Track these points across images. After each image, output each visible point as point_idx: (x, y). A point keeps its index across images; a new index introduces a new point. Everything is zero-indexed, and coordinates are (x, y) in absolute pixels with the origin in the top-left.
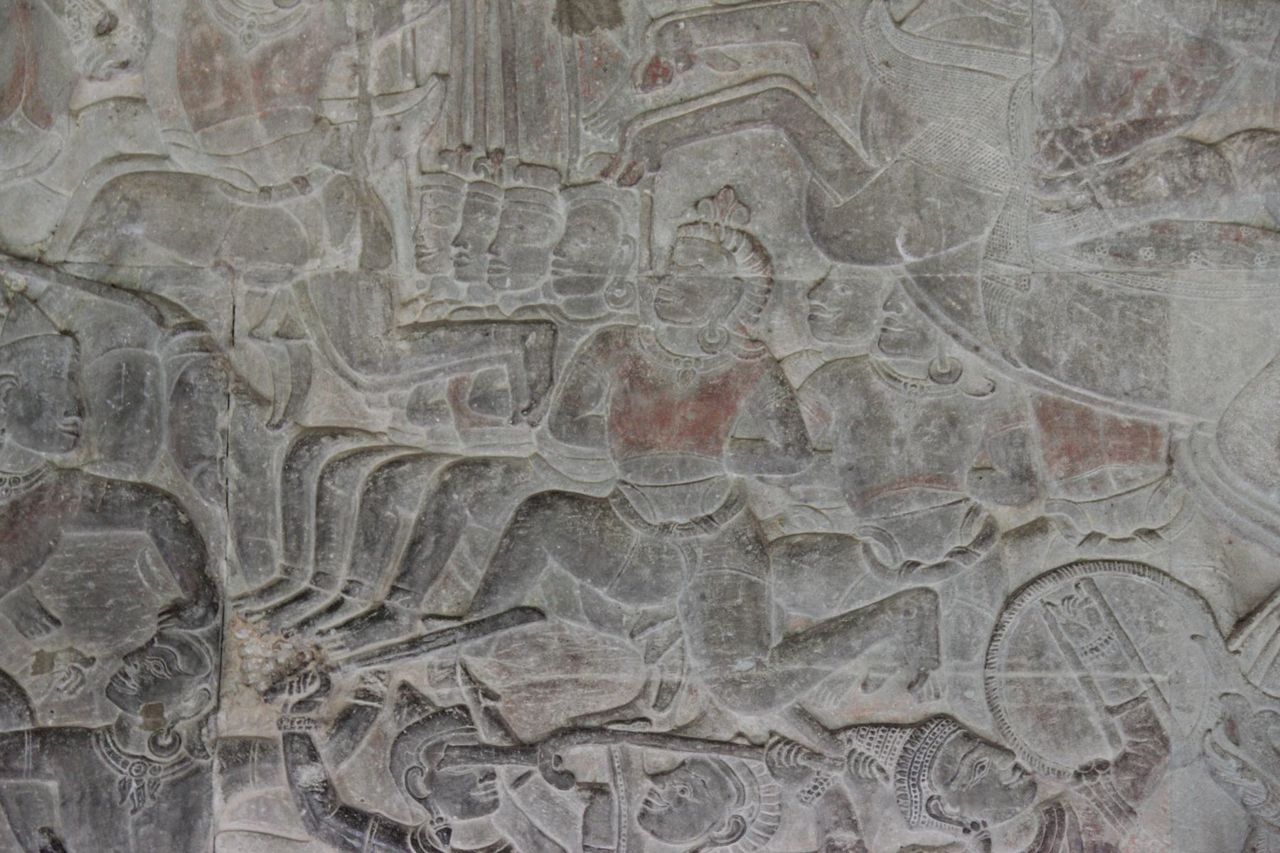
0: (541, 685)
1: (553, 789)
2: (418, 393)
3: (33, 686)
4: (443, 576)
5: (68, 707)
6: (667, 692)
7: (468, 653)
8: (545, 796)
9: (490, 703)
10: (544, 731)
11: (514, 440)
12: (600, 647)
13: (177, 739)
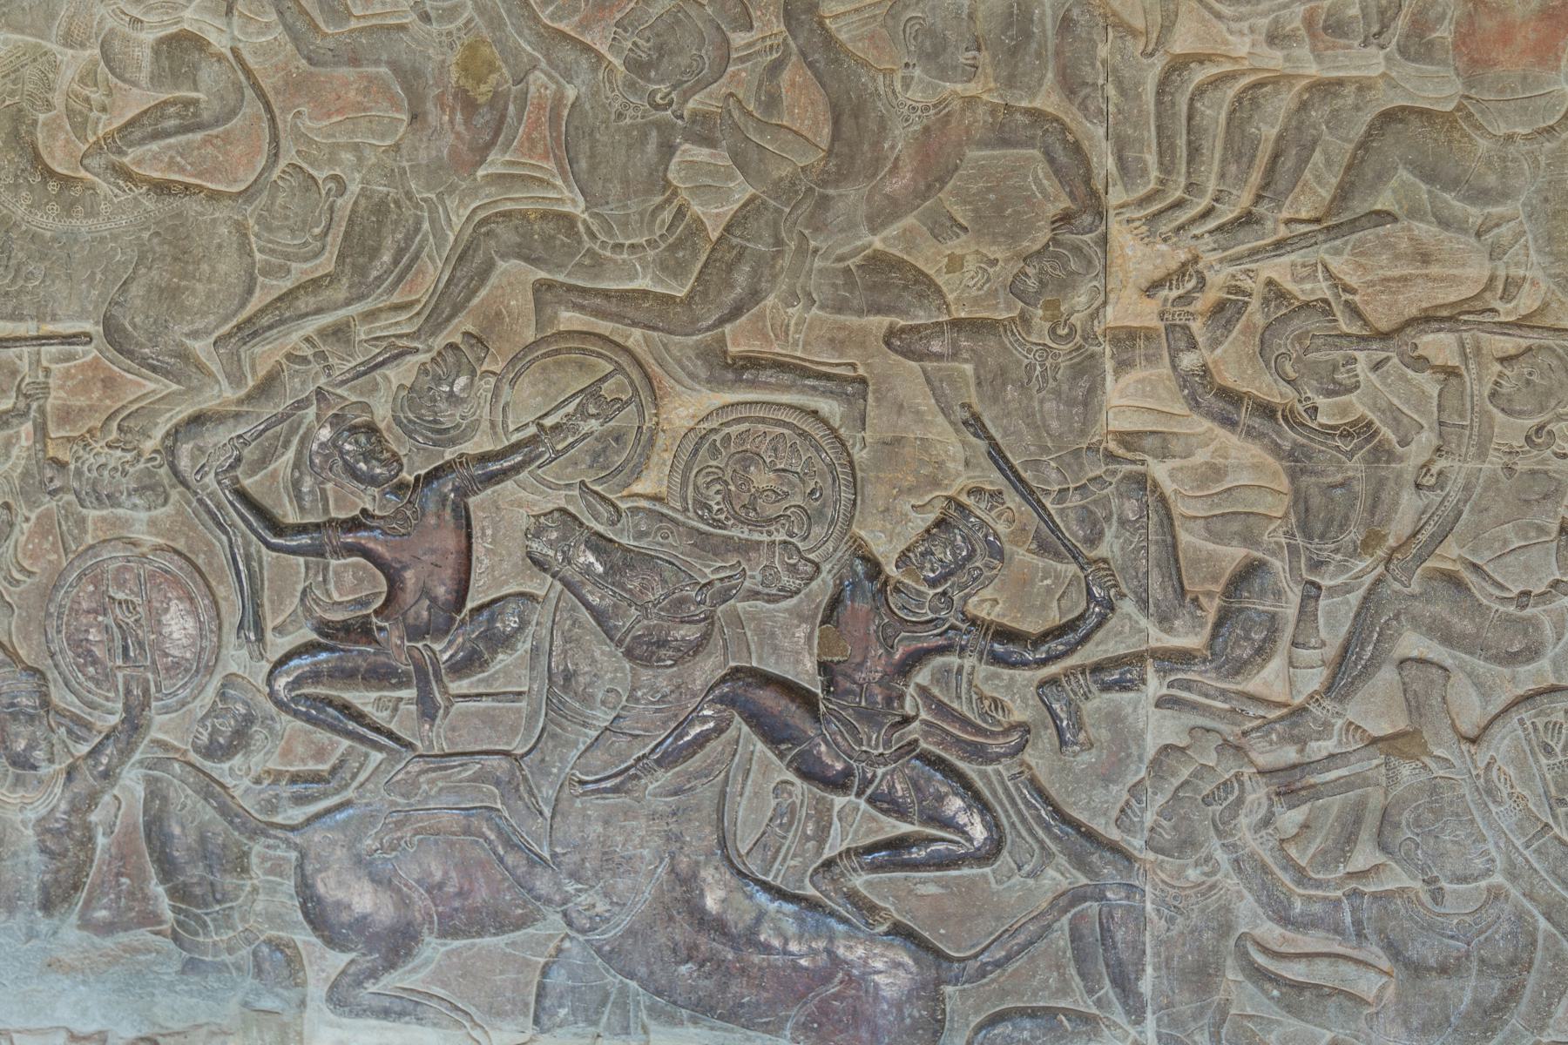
0: (1394, 279)
1: (1410, 373)
2: (1276, 21)
3: (947, 283)
4: (1300, 184)
5: (976, 301)
6: (1511, 287)
7: (1327, 252)
8: (1403, 377)
9: (1350, 297)
10: (1396, 320)
11: (1367, 63)
12: (1447, 246)
13: (1073, 329)
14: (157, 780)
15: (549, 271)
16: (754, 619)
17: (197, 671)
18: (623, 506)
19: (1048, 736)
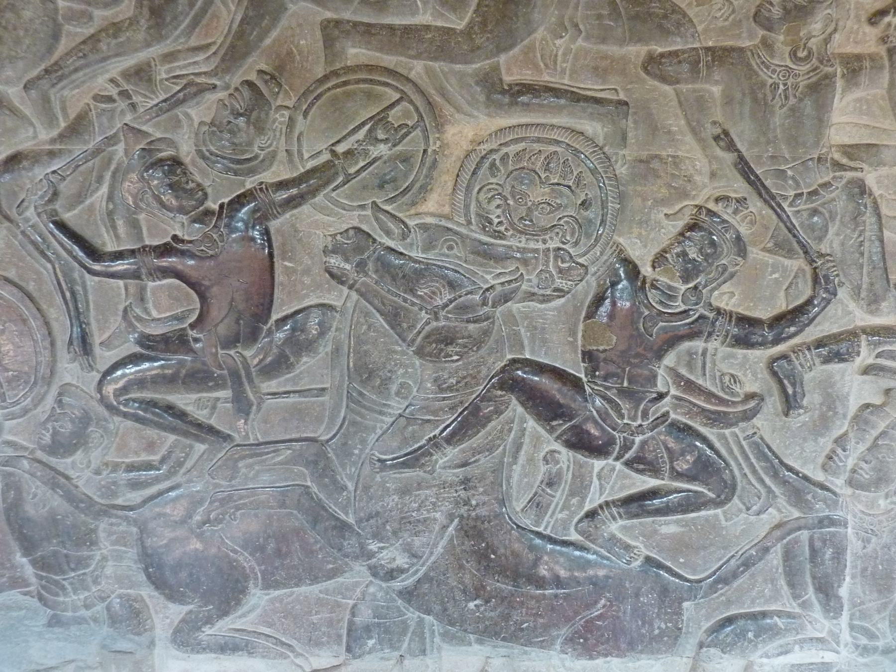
3: (697, 15)
5: (722, 31)
14: (10, 474)
15: (336, 10)
16: (527, 317)
17: (35, 383)
18: (411, 223)
19: (774, 403)
